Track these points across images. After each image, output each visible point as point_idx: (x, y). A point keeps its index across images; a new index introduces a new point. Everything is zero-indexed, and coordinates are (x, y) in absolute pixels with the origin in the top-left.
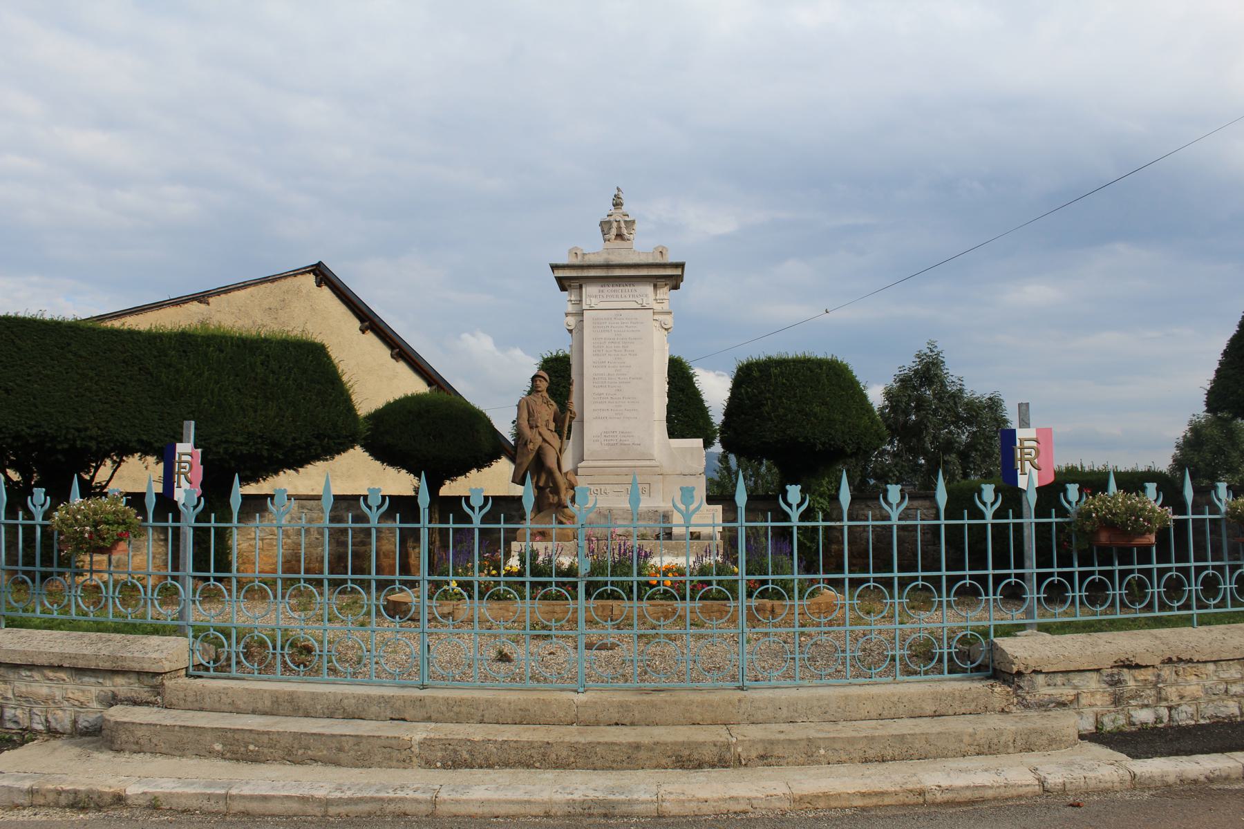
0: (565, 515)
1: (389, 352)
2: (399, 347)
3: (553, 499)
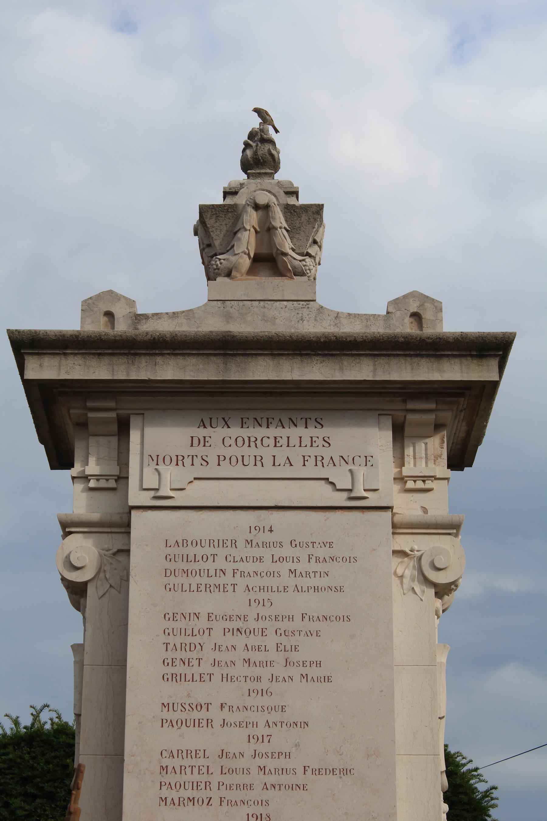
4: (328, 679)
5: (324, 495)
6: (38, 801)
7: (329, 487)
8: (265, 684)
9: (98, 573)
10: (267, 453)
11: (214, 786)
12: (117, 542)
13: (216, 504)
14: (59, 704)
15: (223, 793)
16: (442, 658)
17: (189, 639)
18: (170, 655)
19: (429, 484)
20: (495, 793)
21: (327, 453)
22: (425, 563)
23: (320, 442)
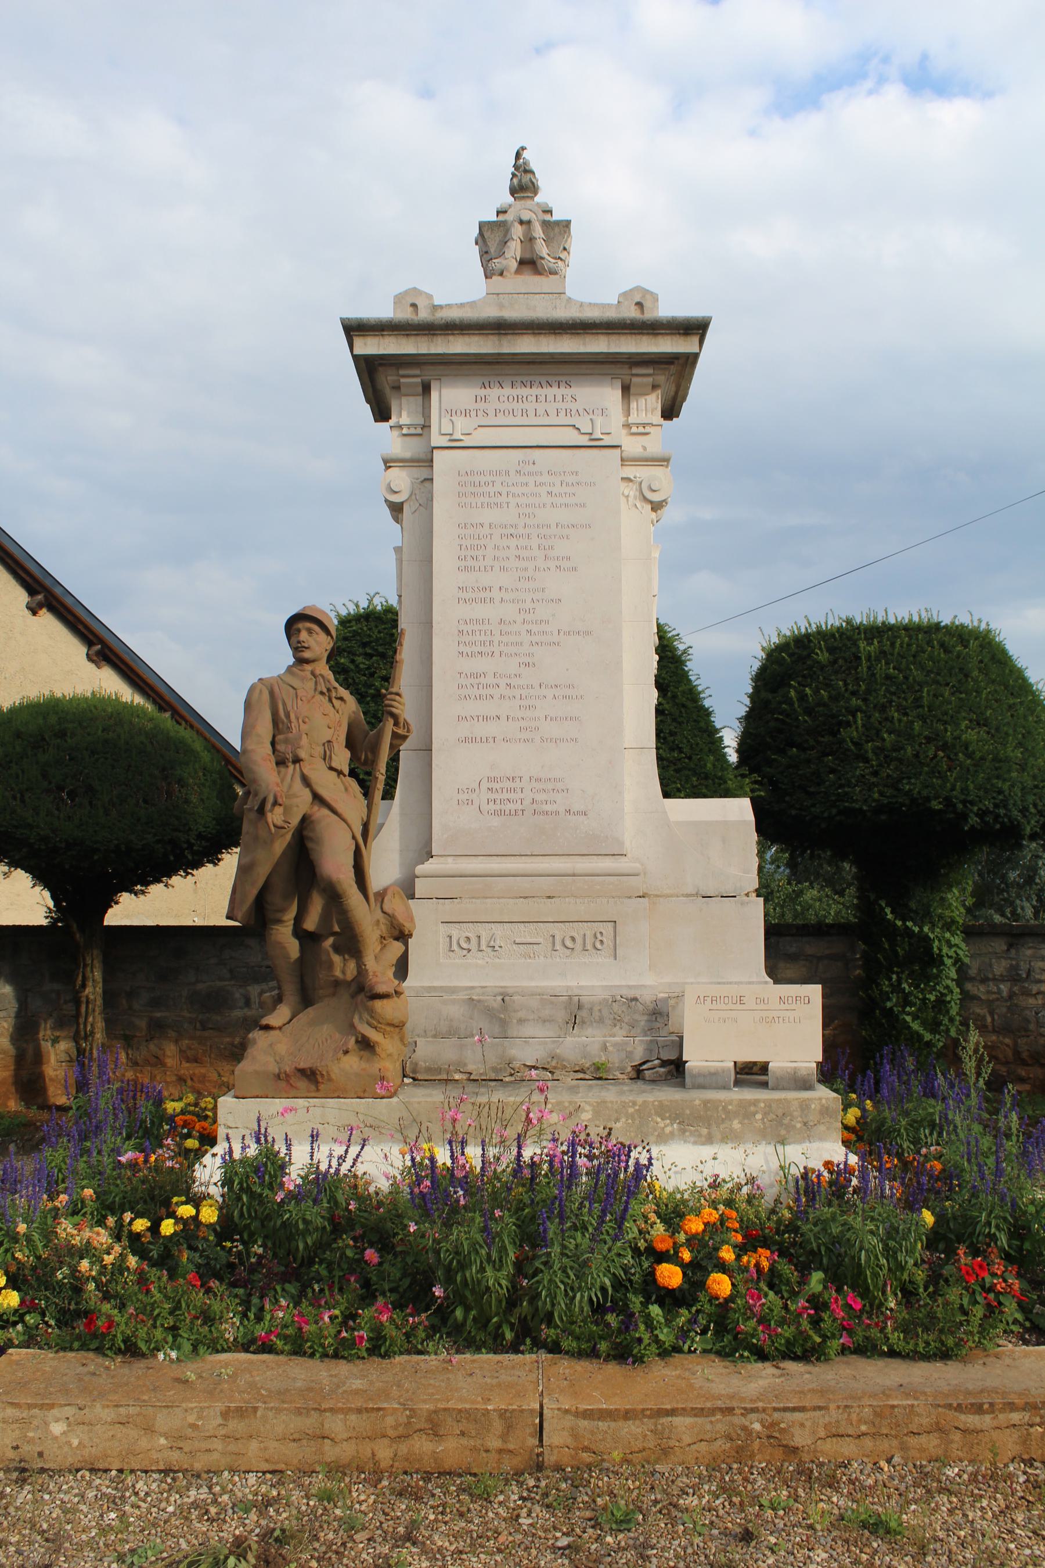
1: (84, 650)
2: (101, 641)
3: (343, 968)
4: (575, 569)
5: (571, 437)
7: (576, 432)
9: (411, 495)
10: (530, 406)
11: (496, 643)
12: (424, 473)
14: (387, 595)
15: (502, 648)
16: (656, 554)
18: (463, 553)
19: (648, 429)
20: (691, 651)
21: (574, 406)
22: (644, 486)
23: (569, 398)
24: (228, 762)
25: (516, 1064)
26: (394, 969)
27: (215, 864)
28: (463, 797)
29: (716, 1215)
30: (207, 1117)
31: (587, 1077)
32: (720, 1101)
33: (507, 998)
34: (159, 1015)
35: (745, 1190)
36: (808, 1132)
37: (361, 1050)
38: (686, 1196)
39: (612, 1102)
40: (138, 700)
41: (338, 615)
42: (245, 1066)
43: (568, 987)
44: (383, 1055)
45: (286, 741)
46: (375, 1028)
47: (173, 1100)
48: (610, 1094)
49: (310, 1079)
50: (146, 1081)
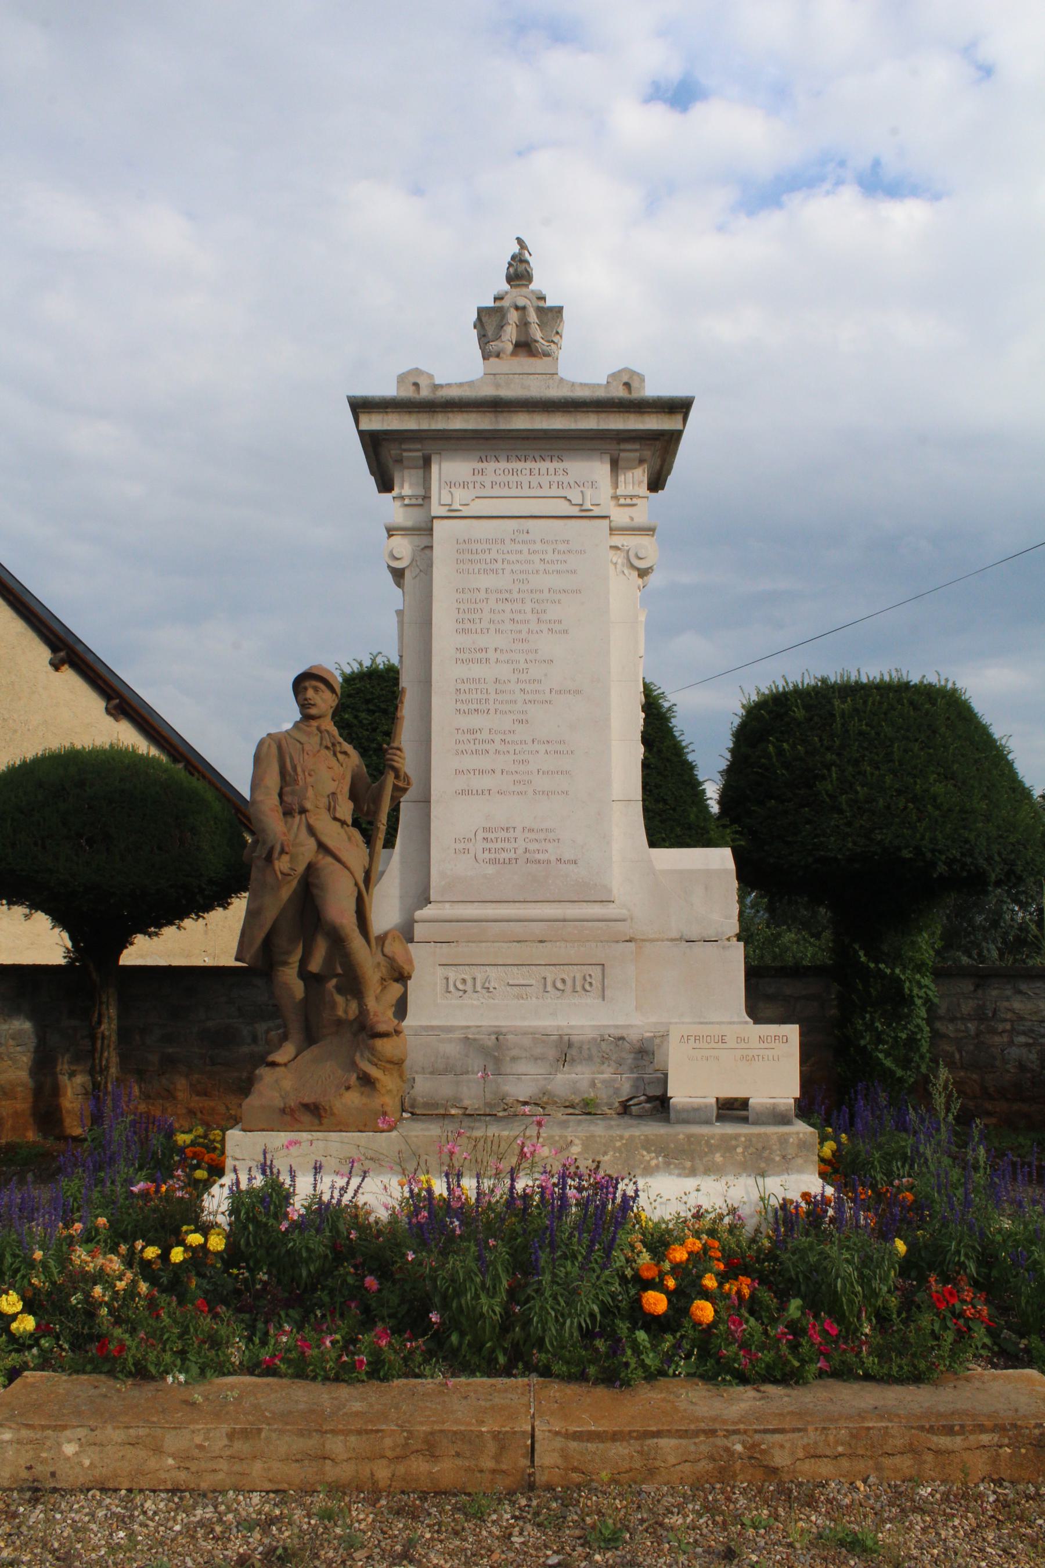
0: (377, 1059)
2: (119, 695)
3: (345, 1007)
4: (566, 632)
6: (377, 714)
7: (567, 503)
8: (524, 635)
10: (525, 479)
11: (491, 702)
12: (424, 541)
13: (490, 514)
15: (497, 706)
16: (642, 618)
17: (473, 606)
18: (461, 616)
19: (635, 501)
20: (675, 708)
22: (632, 554)
24: (238, 810)
25: (510, 1100)
26: (393, 1009)
27: (225, 908)
28: (460, 846)
29: (699, 1245)
30: (215, 1148)
31: (577, 1112)
32: (703, 1136)
33: (501, 1037)
34: (170, 1050)
35: (727, 1220)
36: (786, 1165)
37: (362, 1086)
38: (671, 1226)
39: (600, 1136)
40: (154, 752)
41: (343, 674)
42: (253, 1101)
43: (559, 1027)
44: (383, 1091)
45: (293, 793)
46: (376, 1065)
47: (183, 1132)
48: (598, 1129)
49: (313, 1114)
50: (158, 1113)
